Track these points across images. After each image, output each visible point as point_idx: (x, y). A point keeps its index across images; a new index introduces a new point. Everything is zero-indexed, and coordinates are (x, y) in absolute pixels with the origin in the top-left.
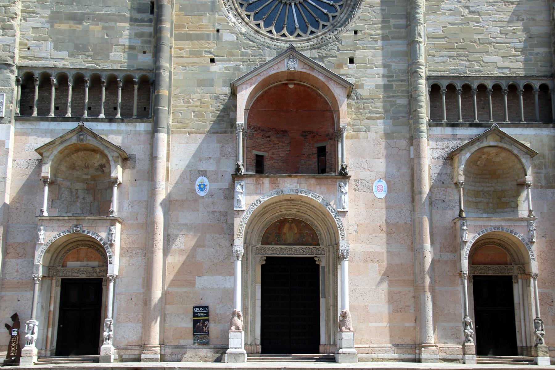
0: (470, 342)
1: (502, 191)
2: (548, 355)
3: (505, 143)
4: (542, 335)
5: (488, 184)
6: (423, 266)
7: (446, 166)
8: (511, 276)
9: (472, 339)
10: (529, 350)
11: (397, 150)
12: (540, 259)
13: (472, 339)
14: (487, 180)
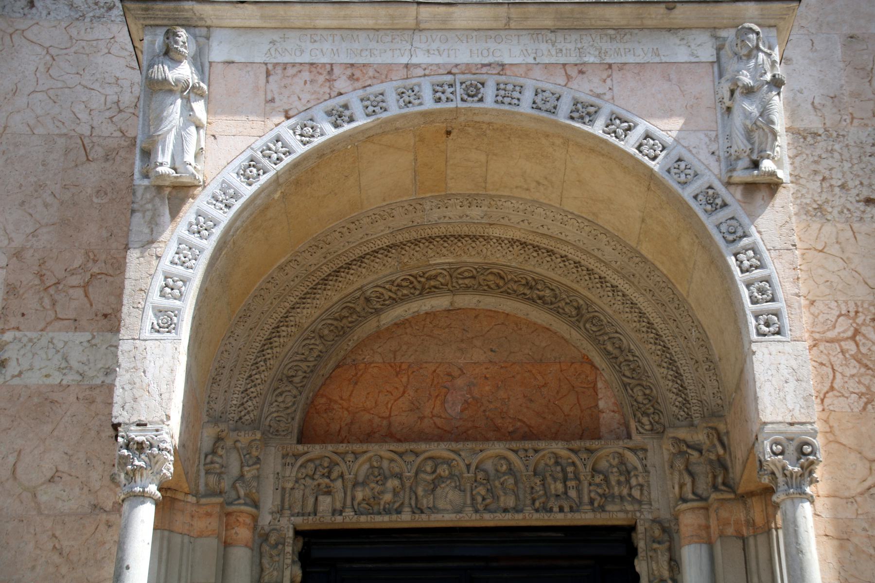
8: (631, 529)
12: (853, 369)
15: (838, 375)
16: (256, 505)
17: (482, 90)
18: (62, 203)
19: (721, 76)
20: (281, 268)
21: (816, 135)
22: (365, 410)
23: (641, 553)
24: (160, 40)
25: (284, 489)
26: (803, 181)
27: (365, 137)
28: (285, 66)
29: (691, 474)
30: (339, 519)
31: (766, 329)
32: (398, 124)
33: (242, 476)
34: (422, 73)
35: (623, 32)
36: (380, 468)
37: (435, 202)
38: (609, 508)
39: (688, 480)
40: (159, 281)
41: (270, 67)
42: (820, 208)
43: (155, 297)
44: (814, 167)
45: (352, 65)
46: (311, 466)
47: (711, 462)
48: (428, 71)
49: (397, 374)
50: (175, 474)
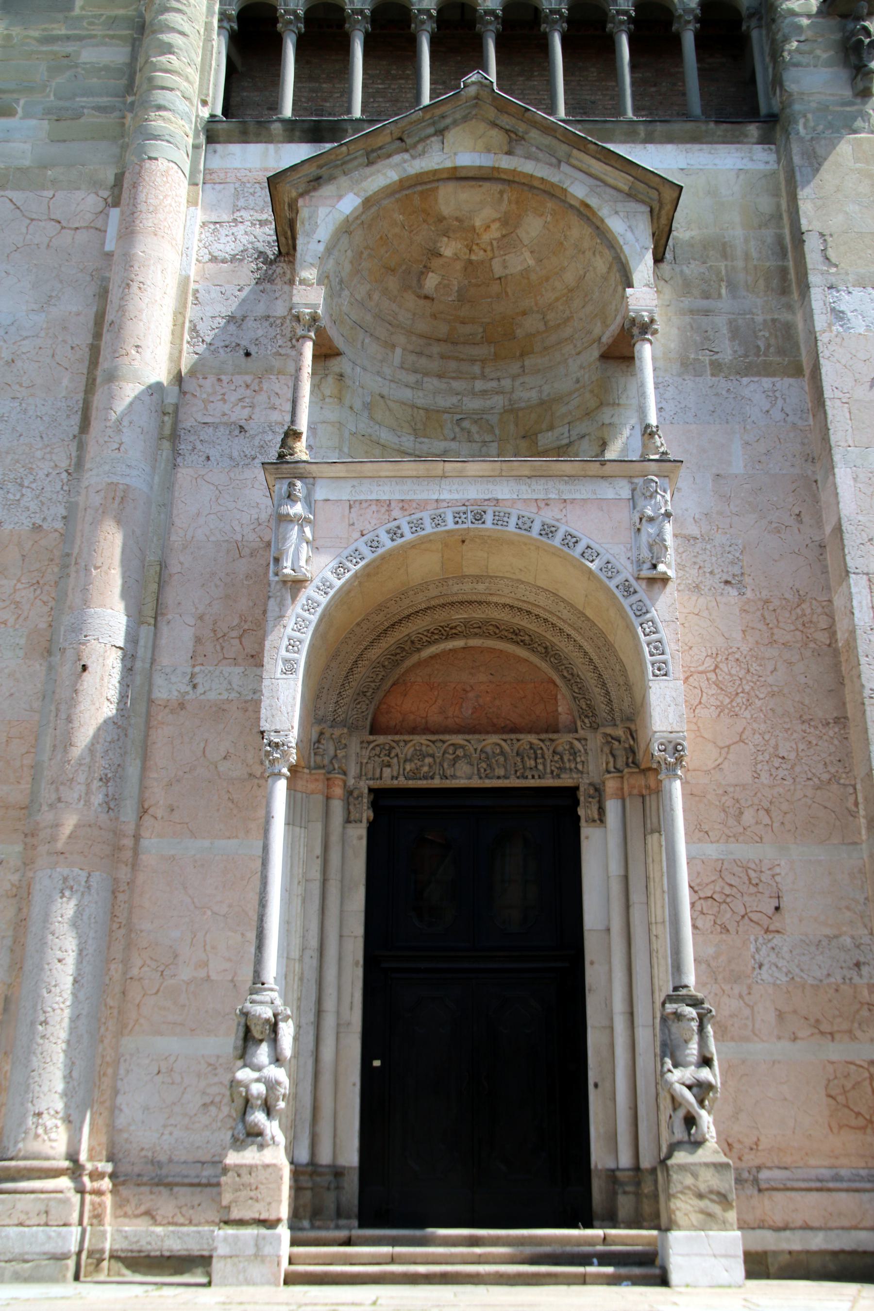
0: (261, 1147)
1: (542, 403)
2: (732, 1216)
3: (528, 157)
4: (702, 1089)
5: (479, 385)
6: (69, 720)
7: (268, 286)
8: (576, 789)
9: (272, 1128)
10: (647, 1189)
11: (52, 228)
12: (714, 690)
13: (272, 1128)
14: (477, 369)
15: (704, 695)
16: (345, 773)
17: (484, 516)
18: (226, 584)
19: (634, 508)
20: (358, 624)
21: (696, 538)
22: (411, 712)
23: (582, 804)
24: (285, 487)
25: (361, 763)
26: (687, 569)
27: (413, 546)
28: (361, 502)
29: (614, 756)
30: (395, 782)
31: (658, 672)
32: (431, 538)
33: (336, 756)
34: (446, 505)
35: (573, 478)
36: (421, 750)
37: (455, 580)
38: (563, 776)
39: (611, 760)
40: (285, 642)
41: (352, 503)
42: (697, 587)
43: (283, 653)
44: (694, 560)
45: (403, 500)
46: (378, 749)
47: (625, 749)
48: (450, 504)
49: (431, 689)
50: (297, 761)
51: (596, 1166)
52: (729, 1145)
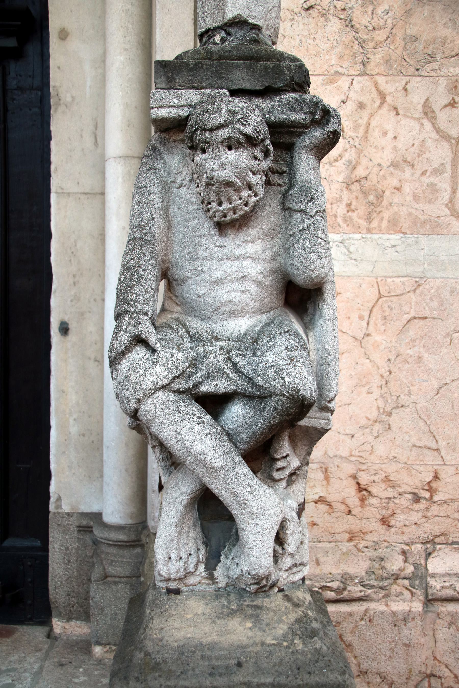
51: (59, 506)
52: (360, 488)
